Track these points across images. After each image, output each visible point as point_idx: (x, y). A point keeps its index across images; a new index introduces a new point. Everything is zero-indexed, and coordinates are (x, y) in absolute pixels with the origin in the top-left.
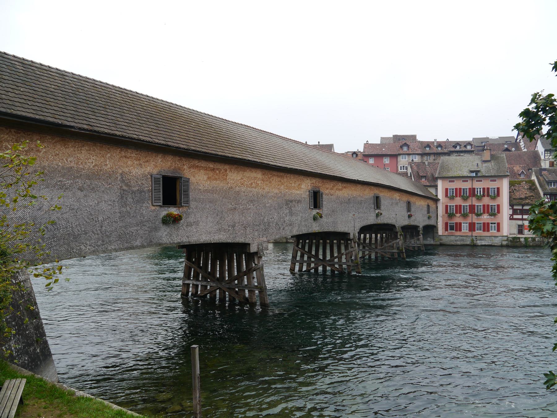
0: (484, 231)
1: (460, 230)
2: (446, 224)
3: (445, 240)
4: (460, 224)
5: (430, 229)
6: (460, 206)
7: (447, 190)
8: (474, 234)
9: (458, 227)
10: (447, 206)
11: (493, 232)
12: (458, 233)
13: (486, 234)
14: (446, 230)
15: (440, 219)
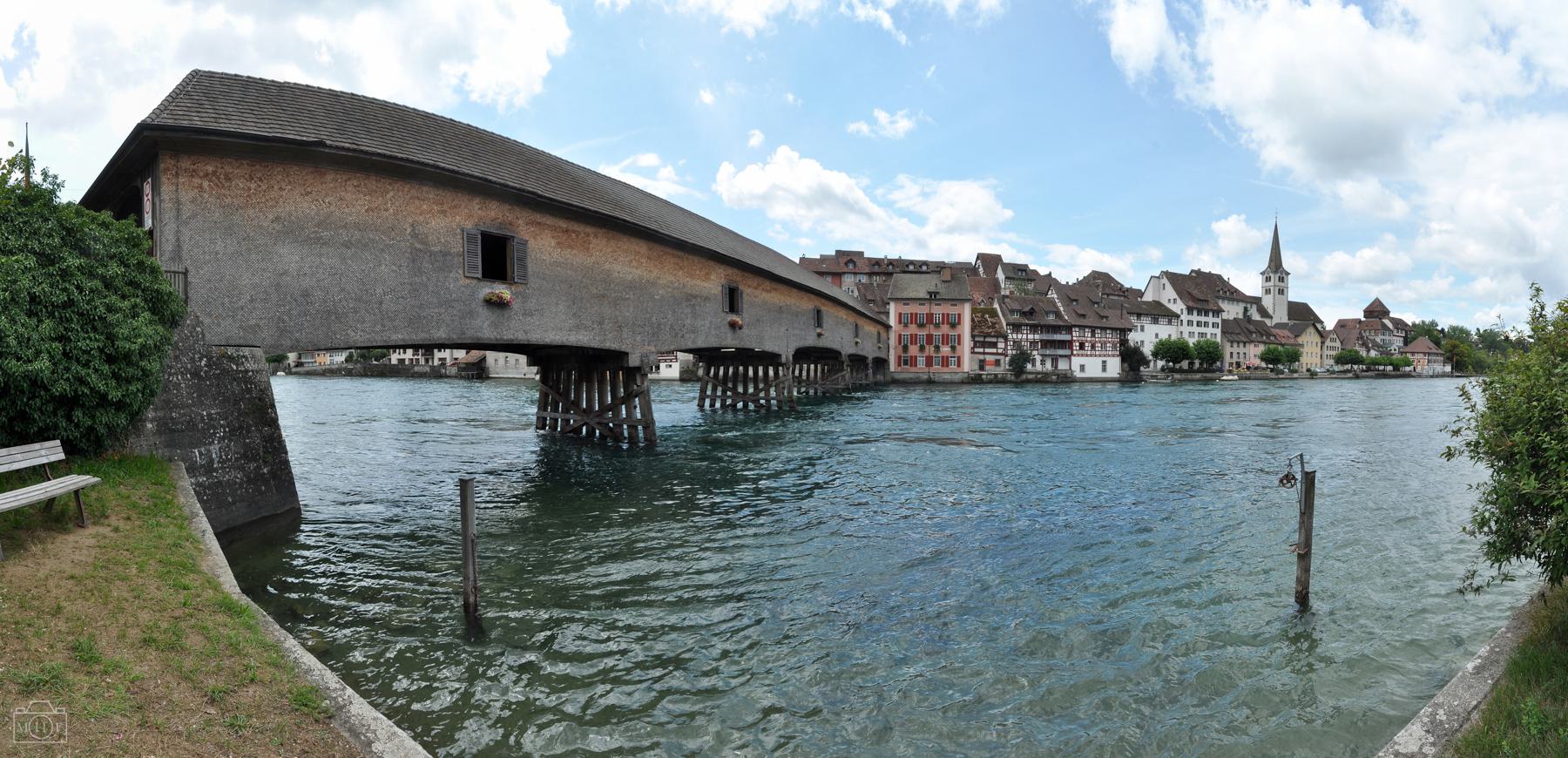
0: (943, 366)
1: (916, 366)
2: (900, 357)
3: (902, 376)
4: (916, 357)
5: (881, 363)
6: (916, 335)
7: (900, 314)
8: (932, 370)
9: (913, 361)
10: (900, 335)
11: (953, 367)
12: (913, 369)
13: (946, 370)
14: (899, 365)
15: (892, 351)
